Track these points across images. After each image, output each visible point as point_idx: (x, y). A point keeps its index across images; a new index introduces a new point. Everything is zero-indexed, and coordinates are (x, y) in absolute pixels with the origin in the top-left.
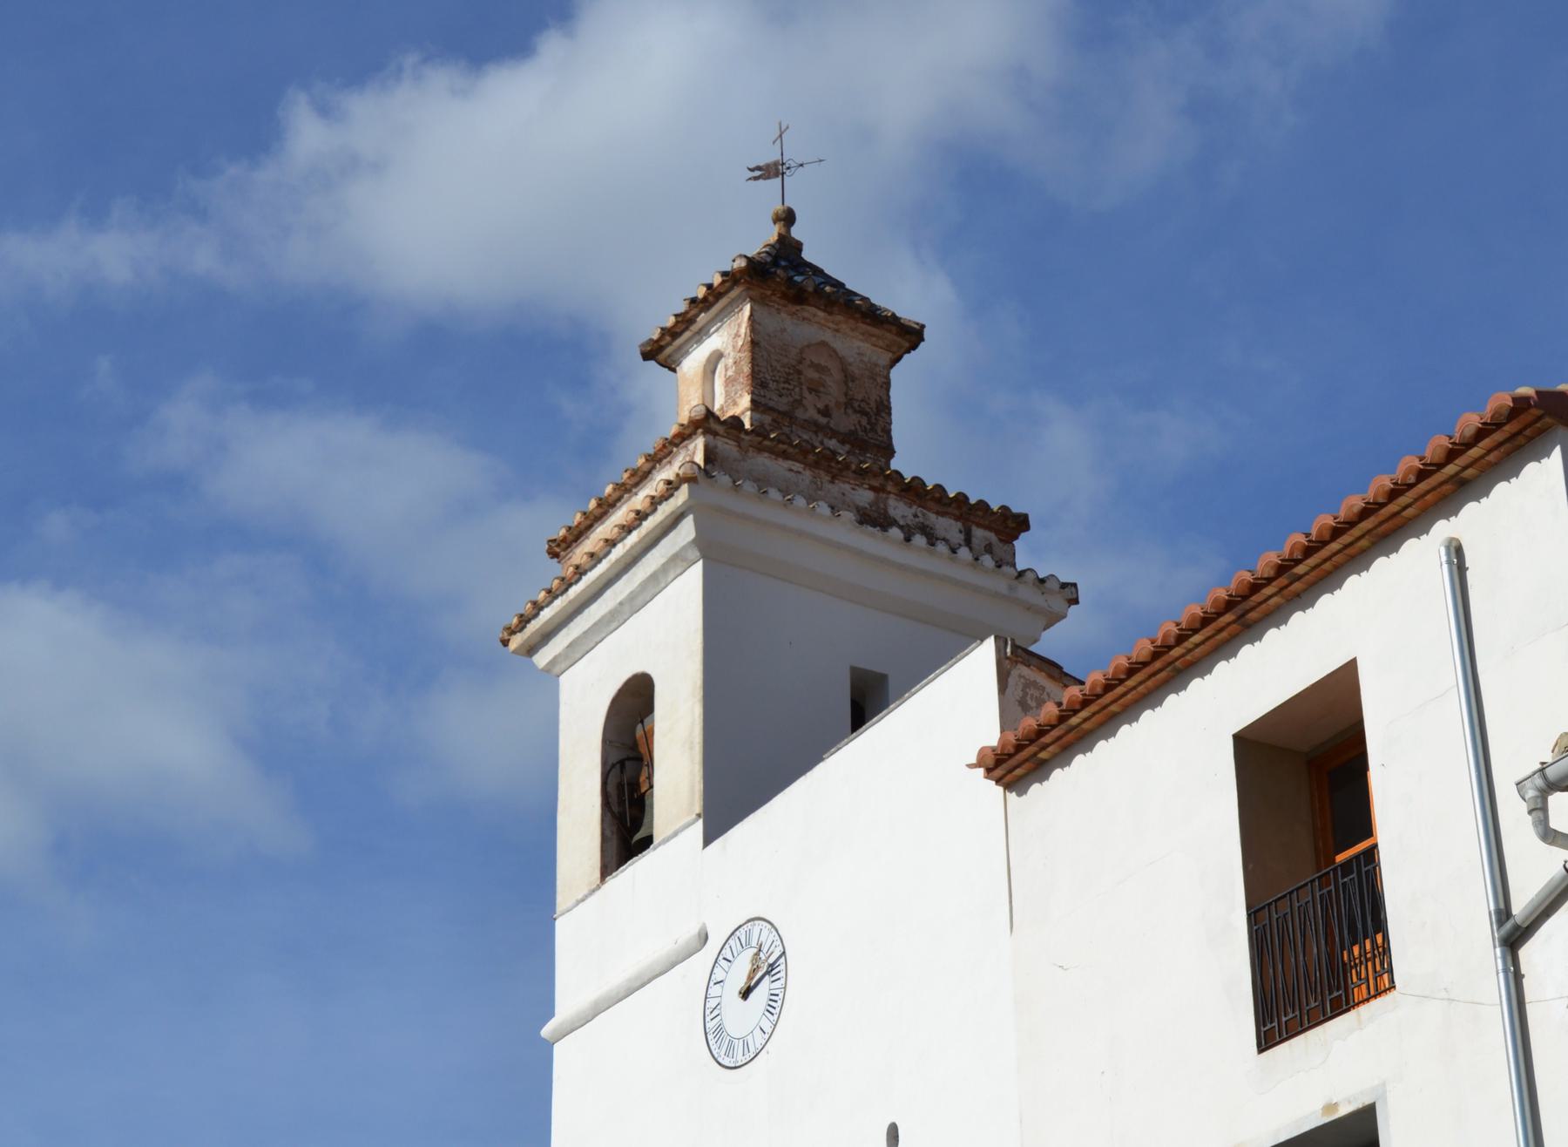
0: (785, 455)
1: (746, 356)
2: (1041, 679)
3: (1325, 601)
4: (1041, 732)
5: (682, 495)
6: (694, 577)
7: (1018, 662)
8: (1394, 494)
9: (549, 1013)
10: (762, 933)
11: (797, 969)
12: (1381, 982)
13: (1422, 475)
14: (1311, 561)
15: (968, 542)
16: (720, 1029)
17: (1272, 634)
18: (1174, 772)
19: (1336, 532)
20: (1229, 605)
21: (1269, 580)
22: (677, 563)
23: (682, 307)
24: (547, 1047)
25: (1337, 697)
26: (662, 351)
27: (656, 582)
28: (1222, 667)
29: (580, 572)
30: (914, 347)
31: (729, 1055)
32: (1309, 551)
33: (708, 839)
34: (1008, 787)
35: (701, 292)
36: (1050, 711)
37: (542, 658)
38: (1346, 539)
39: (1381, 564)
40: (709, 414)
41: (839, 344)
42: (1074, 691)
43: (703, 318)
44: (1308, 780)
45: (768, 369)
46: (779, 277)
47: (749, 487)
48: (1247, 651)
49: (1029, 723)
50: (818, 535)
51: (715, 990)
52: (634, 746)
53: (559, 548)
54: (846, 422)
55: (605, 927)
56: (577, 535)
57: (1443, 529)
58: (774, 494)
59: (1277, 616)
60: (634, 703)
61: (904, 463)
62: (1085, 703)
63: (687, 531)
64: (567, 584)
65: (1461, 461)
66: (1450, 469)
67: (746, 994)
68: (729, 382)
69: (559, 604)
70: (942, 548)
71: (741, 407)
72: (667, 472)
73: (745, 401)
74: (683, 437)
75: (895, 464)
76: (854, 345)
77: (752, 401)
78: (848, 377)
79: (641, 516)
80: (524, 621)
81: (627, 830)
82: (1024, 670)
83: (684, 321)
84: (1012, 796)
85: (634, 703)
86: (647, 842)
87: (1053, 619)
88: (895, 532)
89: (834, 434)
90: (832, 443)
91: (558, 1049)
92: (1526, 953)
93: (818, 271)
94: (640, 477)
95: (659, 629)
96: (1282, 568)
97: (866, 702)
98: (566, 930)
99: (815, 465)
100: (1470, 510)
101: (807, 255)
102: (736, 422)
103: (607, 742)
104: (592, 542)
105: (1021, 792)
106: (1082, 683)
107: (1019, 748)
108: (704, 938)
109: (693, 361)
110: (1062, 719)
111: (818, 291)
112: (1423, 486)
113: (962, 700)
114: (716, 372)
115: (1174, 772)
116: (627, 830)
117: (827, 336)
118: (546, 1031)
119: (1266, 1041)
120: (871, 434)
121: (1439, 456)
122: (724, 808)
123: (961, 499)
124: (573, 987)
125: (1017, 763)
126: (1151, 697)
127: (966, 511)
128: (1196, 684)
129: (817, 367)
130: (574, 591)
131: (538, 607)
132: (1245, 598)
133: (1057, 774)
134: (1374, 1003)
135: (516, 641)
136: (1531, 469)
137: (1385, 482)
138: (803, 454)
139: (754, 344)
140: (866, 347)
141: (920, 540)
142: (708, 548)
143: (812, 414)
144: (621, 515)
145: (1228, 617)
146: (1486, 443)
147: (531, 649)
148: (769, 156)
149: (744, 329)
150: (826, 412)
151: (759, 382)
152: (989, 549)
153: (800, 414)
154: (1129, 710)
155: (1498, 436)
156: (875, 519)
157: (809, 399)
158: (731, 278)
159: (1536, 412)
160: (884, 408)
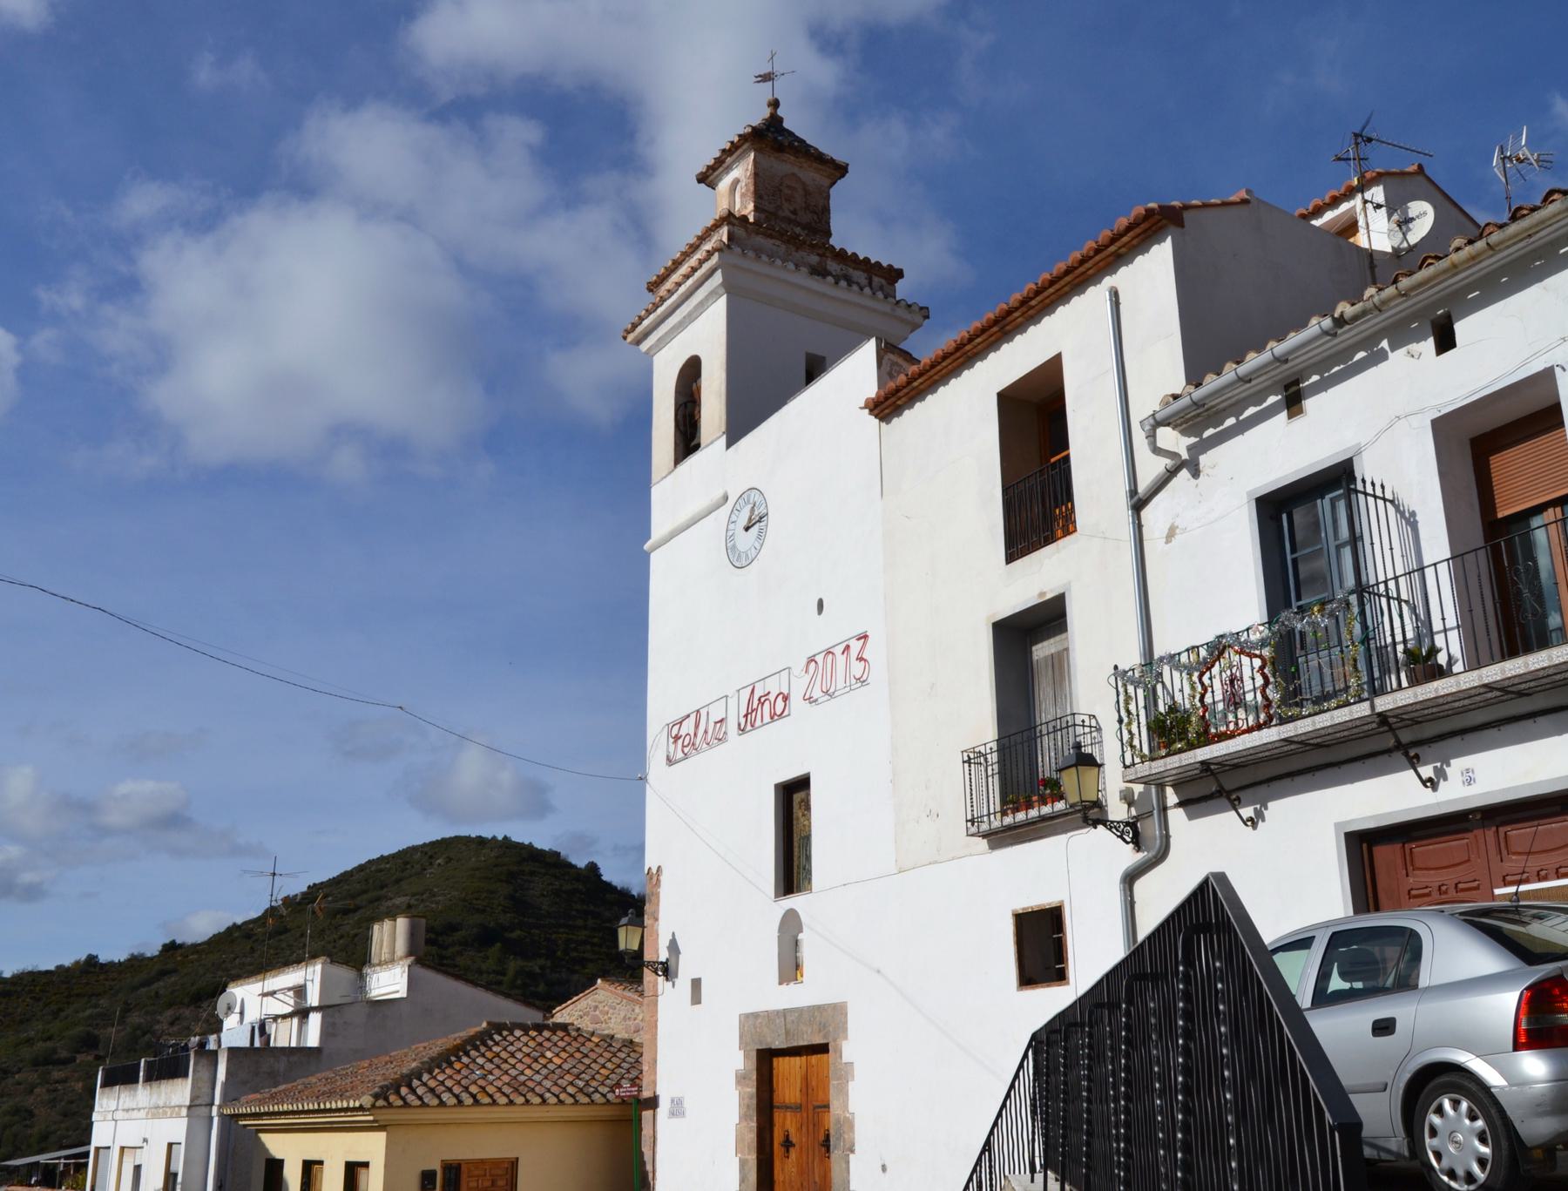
0: (771, 237)
1: (751, 181)
2: (900, 361)
3: (1046, 320)
4: (898, 390)
5: (715, 259)
6: (721, 304)
7: (890, 353)
8: (1083, 261)
9: (647, 535)
10: (755, 496)
11: (772, 519)
12: (1068, 526)
13: (1097, 251)
14: (1039, 298)
15: (870, 284)
16: (734, 546)
17: (1018, 338)
18: (966, 411)
19: (1052, 283)
20: (996, 322)
21: (1017, 309)
22: (713, 296)
23: (718, 154)
24: (647, 556)
25: (1051, 373)
26: (708, 178)
27: (702, 306)
28: (992, 356)
29: (663, 300)
30: (843, 176)
31: (739, 560)
32: (1038, 293)
33: (729, 445)
34: (882, 419)
35: (728, 146)
36: (902, 379)
37: (644, 346)
38: (1057, 286)
39: (1076, 300)
40: (730, 214)
41: (801, 175)
42: (915, 368)
43: (729, 160)
44: (1035, 417)
45: (763, 188)
46: (770, 138)
47: (751, 254)
48: (1005, 347)
49: (892, 385)
50: (790, 281)
51: (732, 526)
52: (692, 395)
53: (653, 287)
54: (805, 218)
55: (677, 491)
56: (662, 279)
57: (1108, 281)
58: (764, 258)
59: (1021, 328)
60: (691, 371)
61: (836, 242)
62: (921, 374)
63: (718, 278)
64: (656, 306)
65: (1118, 244)
66: (1112, 248)
67: (747, 529)
68: (743, 195)
69: (652, 317)
70: (855, 287)
71: (747, 208)
72: (708, 246)
73: (751, 206)
74: (716, 226)
75: (832, 241)
76: (811, 175)
77: (756, 207)
78: (807, 193)
79: (694, 270)
80: (634, 326)
81: (687, 441)
82: (891, 356)
83: (719, 162)
84: (883, 424)
85: (691, 371)
86: (697, 447)
87: (915, 327)
88: (830, 279)
89: (798, 224)
90: (798, 230)
91: (653, 556)
92: (1144, 513)
93: (791, 134)
94: (694, 248)
95: (703, 332)
96: (1024, 302)
97: (814, 369)
98: (656, 492)
99: (788, 242)
100: (1123, 271)
101: (786, 125)
102: (744, 218)
103: (678, 392)
104: (669, 285)
105: (888, 422)
106: (919, 362)
107: (886, 399)
108: (726, 498)
109: (725, 183)
110: (909, 383)
111: (791, 145)
112: (1097, 258)
113: (858, 372)
114: (736, 190)
115: (966, 411)
116: (687, 441)
117: (796, 170)
118: (646, 547)
119: (1011, 558)
120: (819, 225)
121: (1106, 241)
122: (737, 430)
123: (867, 260)
124: (660, 524)
125: (886, 407)
126: (955, 371)
127: (867, 266)
128: (979, 365)
129: (789, 187)
130: (660, 310)
131: (641, 319)
132: (1004, 318)
133: (907, 412)
134: (1068, 538)
135: (631, 337)
136: (1155, 248)
137: (1077, 255)
138: (781, 235)
139: (757, 175)
140: (817, 176)
141: (843, 283)
142: (729, 287)
143: (787, 213)
144: (684, 269)
145: (995, 329)
146: (1131, 234)
147: (638, 342)
148: (766, 69)
149: (750, 167)
150: (794, 212)
151: (759, 196)
152: (881, 288)
153: (780, 213)
154: (944, 379)
155: (1138, 230)
156: (819, 272)
157: (786, 205)
158: (743, 138)
159: (1157, 217)
160: (826, 210)
